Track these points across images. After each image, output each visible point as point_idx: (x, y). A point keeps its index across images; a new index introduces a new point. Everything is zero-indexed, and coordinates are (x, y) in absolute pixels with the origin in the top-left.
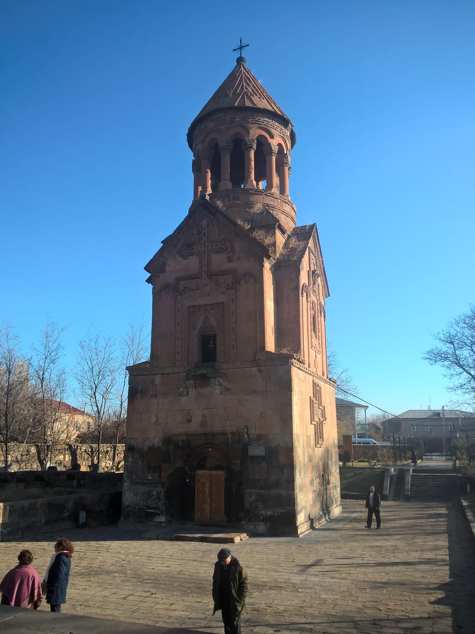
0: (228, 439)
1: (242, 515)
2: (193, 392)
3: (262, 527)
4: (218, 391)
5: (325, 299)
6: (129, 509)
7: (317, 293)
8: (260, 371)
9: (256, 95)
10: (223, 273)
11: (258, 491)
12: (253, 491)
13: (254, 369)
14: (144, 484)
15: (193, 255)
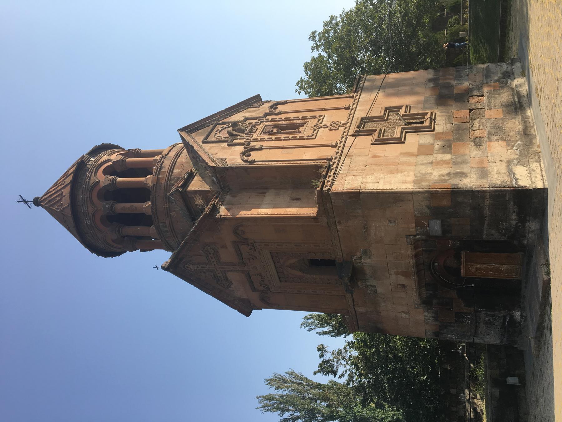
0: (423, 250)
1: (516, 242)
2: (372, 282)
3: (533, 225)
4: (368, 261)
5: (263, 100)
6: (505, 339)
7: (254, 121)
8: (339, 223)
9: (61, 199)
10: (239, 253)
11: (485, 227)
12: (485, 232)
13: (338, 227)
14: (476, 327)
15: (227, 277)
